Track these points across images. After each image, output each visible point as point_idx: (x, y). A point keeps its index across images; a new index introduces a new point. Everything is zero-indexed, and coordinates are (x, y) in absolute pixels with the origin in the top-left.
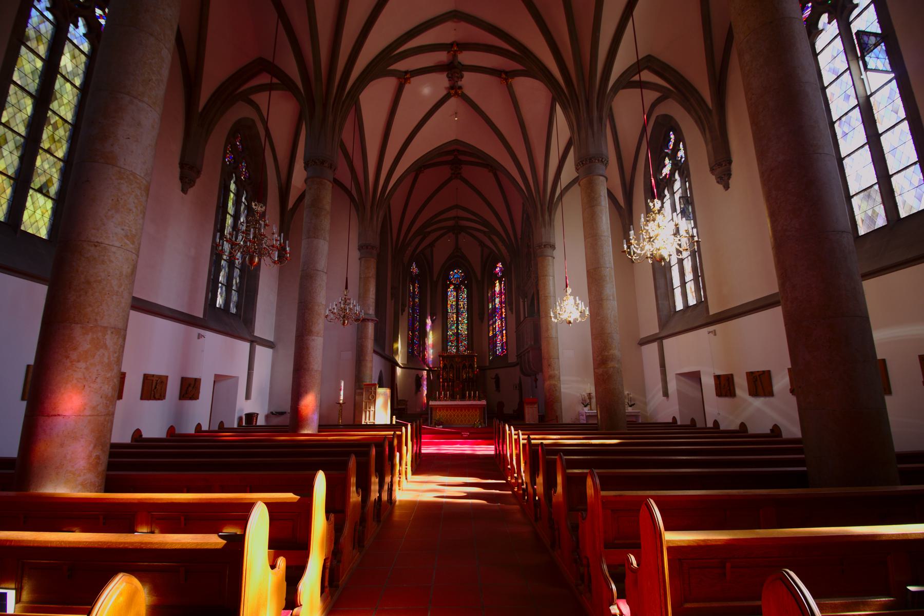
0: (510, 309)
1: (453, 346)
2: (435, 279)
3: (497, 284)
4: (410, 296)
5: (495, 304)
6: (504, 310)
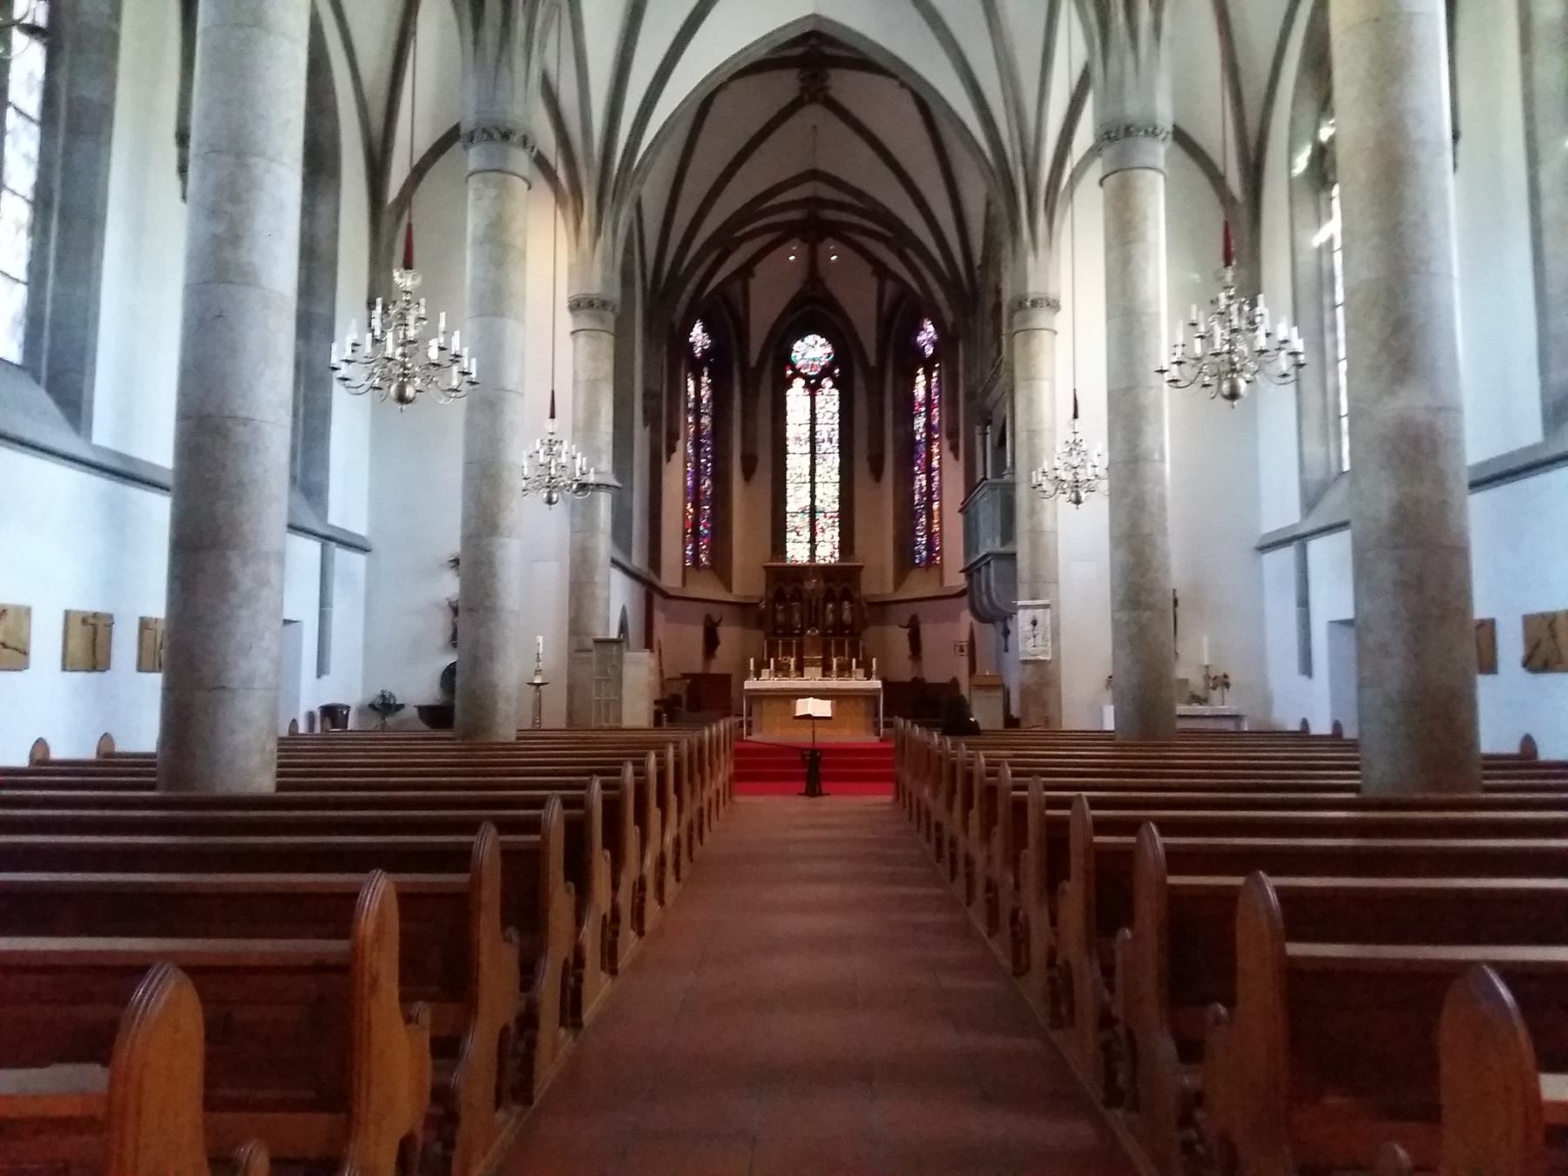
3: (921, 379)
6: (935, 450)
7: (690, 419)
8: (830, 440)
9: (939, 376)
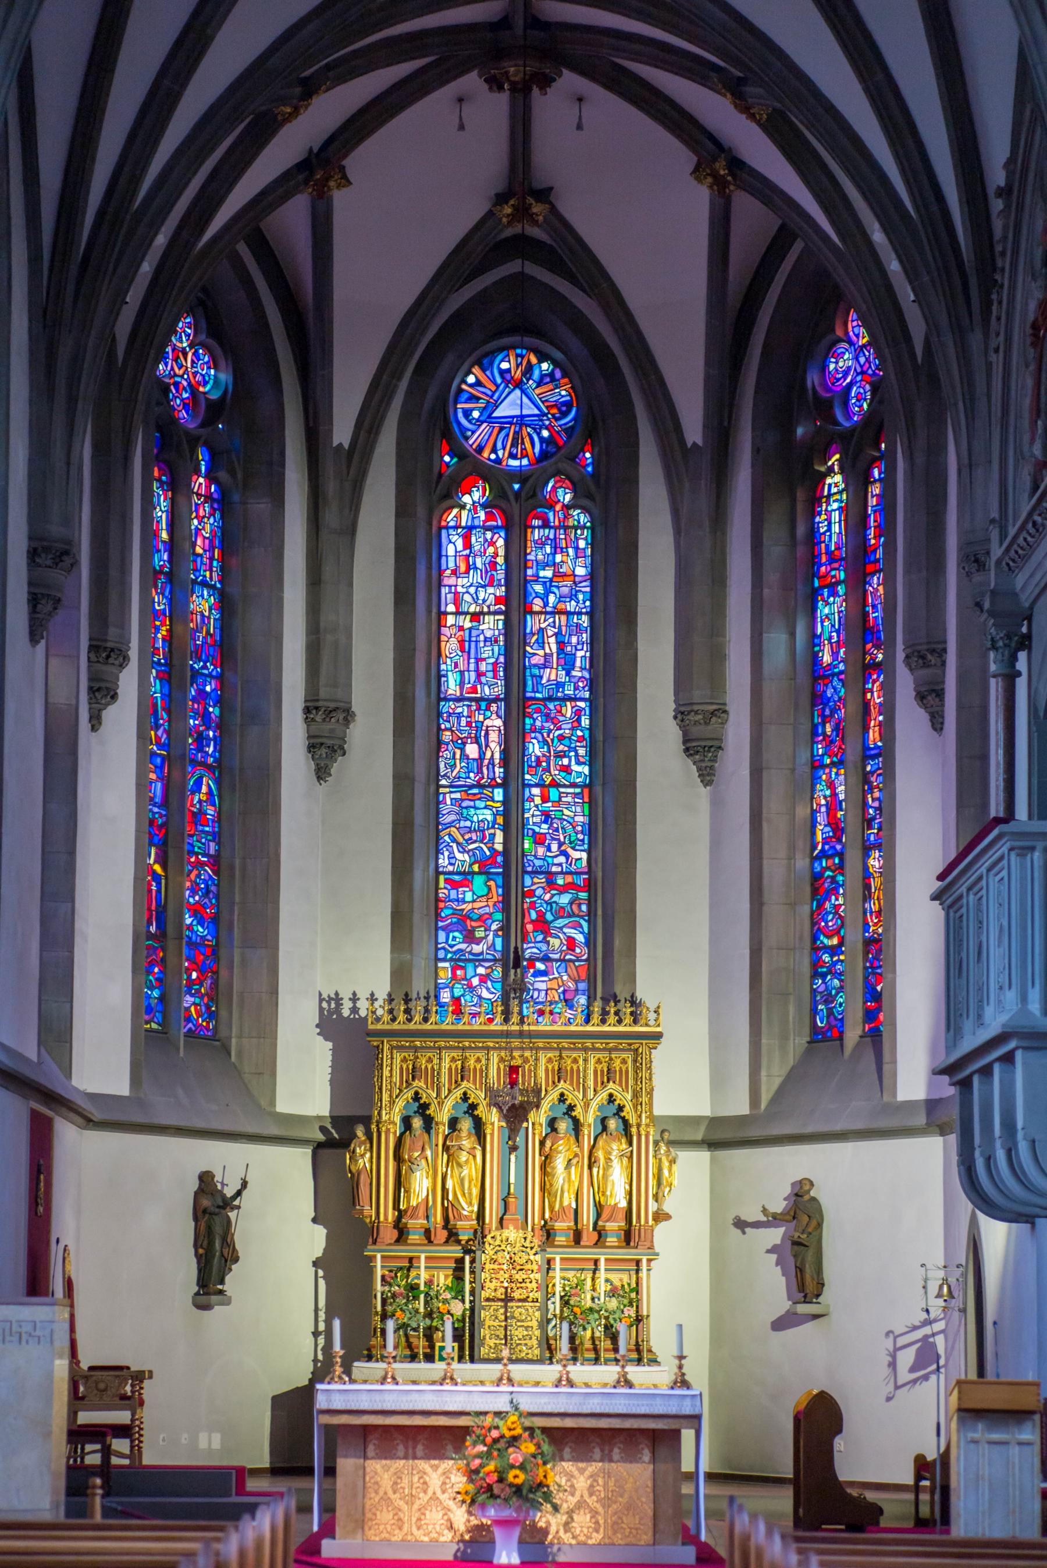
0: (920, 698)
1: (478, 960)
2: (342, 433)
4: (150, 576)
5: (814, 639)
7: (160, 604)
8: (568, 666)
9: (888, 483)
